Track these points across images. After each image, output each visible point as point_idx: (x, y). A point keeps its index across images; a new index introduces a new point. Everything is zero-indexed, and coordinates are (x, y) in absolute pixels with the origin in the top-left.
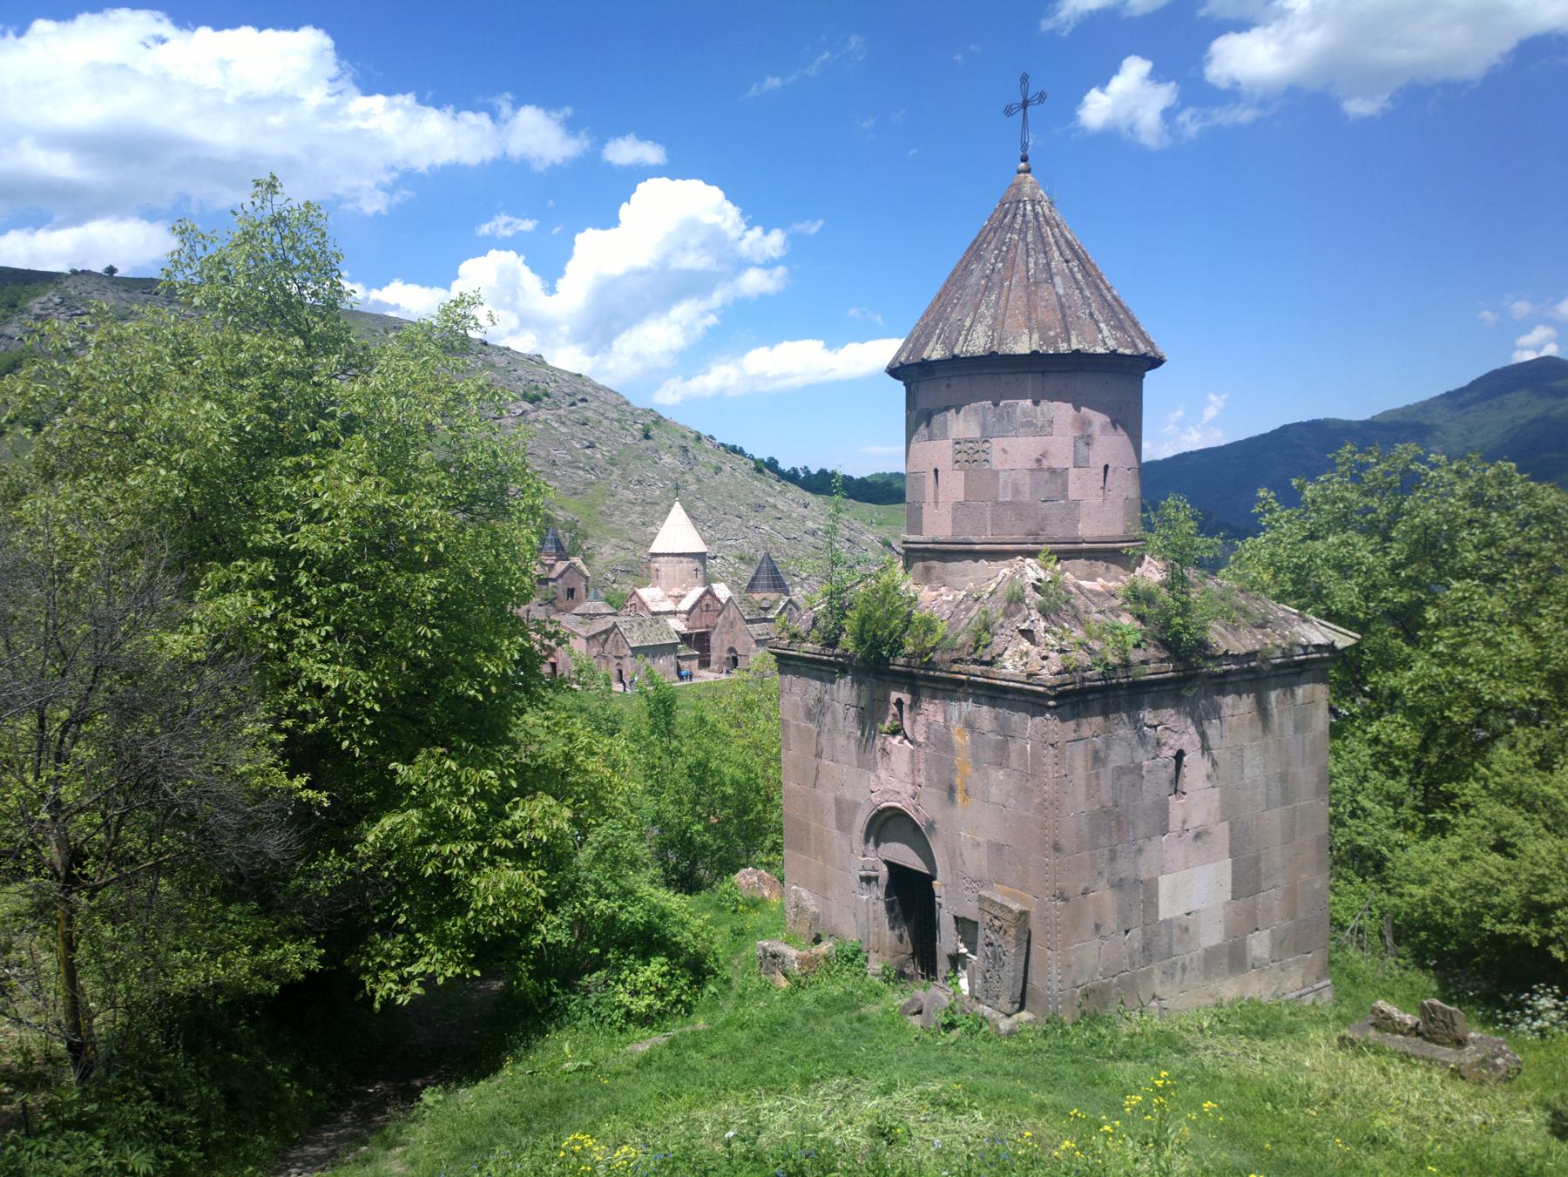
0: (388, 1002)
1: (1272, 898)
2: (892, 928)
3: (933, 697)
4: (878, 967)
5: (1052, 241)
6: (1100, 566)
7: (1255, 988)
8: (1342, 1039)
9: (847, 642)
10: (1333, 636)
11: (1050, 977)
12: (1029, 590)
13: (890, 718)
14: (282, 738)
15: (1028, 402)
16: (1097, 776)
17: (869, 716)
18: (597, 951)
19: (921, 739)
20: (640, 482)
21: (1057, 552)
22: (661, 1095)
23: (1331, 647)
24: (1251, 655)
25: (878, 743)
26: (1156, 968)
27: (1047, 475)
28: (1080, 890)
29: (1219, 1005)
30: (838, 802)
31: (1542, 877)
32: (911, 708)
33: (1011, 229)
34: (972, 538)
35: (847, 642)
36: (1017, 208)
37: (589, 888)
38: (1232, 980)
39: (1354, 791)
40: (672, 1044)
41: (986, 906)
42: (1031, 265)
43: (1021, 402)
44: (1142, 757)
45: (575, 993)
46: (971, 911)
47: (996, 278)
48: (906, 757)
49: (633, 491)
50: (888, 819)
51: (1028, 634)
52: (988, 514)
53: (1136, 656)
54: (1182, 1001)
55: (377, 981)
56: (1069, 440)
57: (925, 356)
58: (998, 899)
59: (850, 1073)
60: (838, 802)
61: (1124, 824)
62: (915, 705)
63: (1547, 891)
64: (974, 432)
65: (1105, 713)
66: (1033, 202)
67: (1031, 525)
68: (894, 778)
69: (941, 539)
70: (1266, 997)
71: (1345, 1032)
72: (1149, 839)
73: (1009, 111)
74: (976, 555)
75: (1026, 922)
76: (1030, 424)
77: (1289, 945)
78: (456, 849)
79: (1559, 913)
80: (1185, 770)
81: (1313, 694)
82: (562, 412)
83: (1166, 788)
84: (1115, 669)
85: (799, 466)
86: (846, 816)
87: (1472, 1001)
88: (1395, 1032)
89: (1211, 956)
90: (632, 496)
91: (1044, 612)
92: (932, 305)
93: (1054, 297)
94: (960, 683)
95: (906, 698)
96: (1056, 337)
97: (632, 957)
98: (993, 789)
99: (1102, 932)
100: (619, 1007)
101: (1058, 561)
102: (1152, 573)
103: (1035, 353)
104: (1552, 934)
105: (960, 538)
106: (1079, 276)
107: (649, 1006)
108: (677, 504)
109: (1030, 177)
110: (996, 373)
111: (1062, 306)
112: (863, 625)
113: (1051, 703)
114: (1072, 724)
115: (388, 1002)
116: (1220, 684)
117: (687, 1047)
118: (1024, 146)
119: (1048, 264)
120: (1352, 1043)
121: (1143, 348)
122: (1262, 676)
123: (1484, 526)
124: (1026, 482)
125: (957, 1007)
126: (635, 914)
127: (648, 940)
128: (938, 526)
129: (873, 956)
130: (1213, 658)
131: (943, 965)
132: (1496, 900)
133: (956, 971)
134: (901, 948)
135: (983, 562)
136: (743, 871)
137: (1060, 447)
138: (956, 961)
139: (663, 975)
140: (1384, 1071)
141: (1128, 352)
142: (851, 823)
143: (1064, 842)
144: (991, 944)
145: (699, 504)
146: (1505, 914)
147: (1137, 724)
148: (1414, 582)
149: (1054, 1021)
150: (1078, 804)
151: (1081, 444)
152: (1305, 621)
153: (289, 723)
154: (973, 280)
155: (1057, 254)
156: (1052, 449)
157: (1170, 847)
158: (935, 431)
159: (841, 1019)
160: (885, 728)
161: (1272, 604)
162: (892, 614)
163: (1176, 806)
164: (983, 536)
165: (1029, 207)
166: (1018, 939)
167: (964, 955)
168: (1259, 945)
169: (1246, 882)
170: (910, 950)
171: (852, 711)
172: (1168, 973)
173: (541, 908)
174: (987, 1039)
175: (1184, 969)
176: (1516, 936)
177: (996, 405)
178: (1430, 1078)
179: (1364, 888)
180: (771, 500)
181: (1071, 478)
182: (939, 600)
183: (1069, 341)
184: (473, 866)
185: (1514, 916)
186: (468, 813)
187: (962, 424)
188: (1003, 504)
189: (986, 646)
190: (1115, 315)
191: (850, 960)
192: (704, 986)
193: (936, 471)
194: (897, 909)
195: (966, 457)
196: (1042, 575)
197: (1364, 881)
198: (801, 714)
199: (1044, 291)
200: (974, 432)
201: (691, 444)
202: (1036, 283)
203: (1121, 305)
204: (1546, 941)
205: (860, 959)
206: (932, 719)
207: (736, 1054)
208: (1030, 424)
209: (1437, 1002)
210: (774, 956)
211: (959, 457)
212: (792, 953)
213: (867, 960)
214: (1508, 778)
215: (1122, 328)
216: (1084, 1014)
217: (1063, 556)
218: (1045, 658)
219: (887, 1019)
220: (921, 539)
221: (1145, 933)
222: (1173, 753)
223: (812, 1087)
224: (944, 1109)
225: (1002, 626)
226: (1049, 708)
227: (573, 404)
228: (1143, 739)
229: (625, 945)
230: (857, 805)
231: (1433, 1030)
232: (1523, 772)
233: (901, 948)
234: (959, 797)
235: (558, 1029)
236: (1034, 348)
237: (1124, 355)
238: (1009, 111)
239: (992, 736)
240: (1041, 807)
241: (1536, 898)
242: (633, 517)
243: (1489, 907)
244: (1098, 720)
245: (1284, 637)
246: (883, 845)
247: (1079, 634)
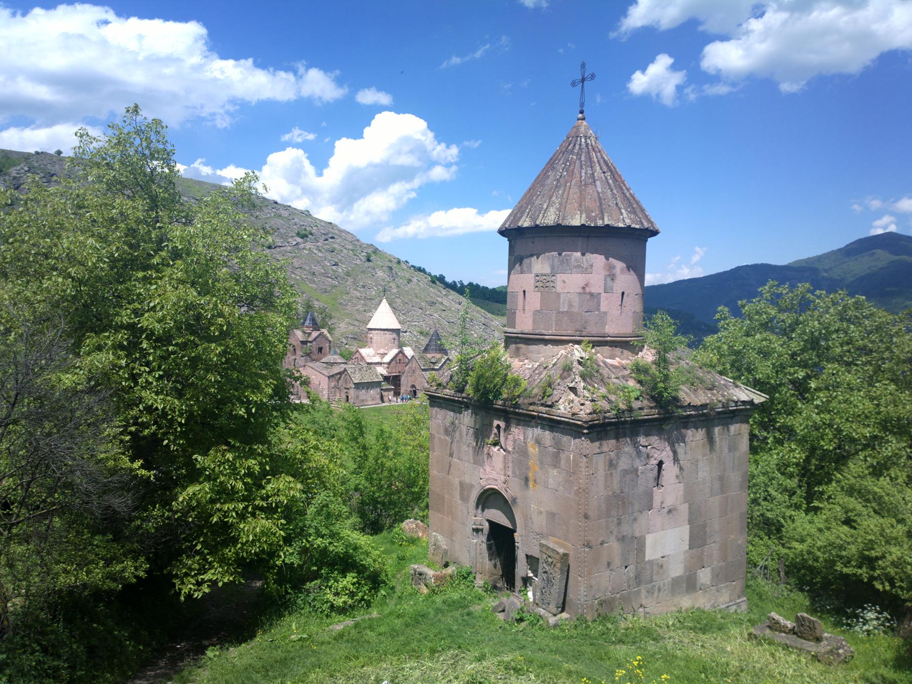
0: (189, 596)
1: (713, 548)
2: (490, 560)
3: (518, 425)
4: (481, 583)
5: (596, 160)
6: (618, 351)
7: (702, 601)
8: (750, 634)
9: (469, 390)
10: (753, 396)
11: (579, 592)
12: (575, 364)
13: (493, 436)
14: (128, 438)
15: (579, 254)
16: (611, 474)
17: (481, 434)
18: (315, 568)
19: (510, 449)
20: (364, 287)
21: (592, 342)
22: (347, 657)
23: (751, 402)
24: (704, 406)
25: (486, 450)
26: (643, 588)
27: (588, 297)
28: (600, 541)
29: (680, 612)
30: (461, 484)
31: (871, 540)
32: (505, 430)
33: (572, 152)
34: (544, 332)
35: (469, 390)
36: (576, 140)
37: (312, 531)
38: (688, 596)
39: (766, 485)
40: (356, 626)
41: (544, 550)
42: (583, 174)
43: (575, 254)
44: (639, 464)
45: (301, 593)
46: (535, 552)
48: (501, 459)
50: (490, 495)
51: (573, 390)
53: (636, 405)
54: (658, 609)
55: (183, 583)
57: (520, 224)
58: (551, 546)
59: (460, 647)
60: (461, 484)
61: (627, 504)
62: (507, 428)
63: (873, 549)
64: (547, 270)
65: (617, 438)
66: (586, 137)
68: (493, 472)
69: (526, 331)
70: (707, 607)
71: (752, 630)
72: (641, 512)
73: (574, 84)
74: (546, 342)
75: (567, 560)
76: (579, 266)
79: (880, 562)
80: (663, 472)
81: (740, 430)
82: (319, 244)
83: (652, 483)
84: (623, 412)
85: (457, 280)
86: (466, 493)
87: (829, 612)
89: (676, 582)
90: (359, 294)
91: (583, 377)
92: (525, 195)
93: (596, 193)
94: (533, 417)
95: (502, 424)
96: (596, 216)
97: (336, 572)
98: (551, 481)
99: (612, 567)
100: (327, 602)
101: (593, 347)
102: (648, 356)
103: (583, 225)
104: (876, 575)
105: (537, 332)
106: (611, 181)
107: (345, 602)
108: (384, 300)
109: (584, 123)
110: (560, 236)
111: (600, 199)
112: (479, 380)
113: (585, 431)
114: (597, 444)
115: (189, 596)
116: (685, 422)
117: (365, 628)
118: (582, 105)
119: (593, 174)
120: (756, 638)
121: (646, 225)
122: (711, 418)
123: (846, 333)
124: (576, 300)
125: (525, 609)
126: (338, 548)
127: (346, 563)
128: (524, 324)
129: (478, 576)
130: (682, 407)
131: (519, 583)
132: (844, 553)
133: (526, 587)
134: (495, 571)
135: (550, 346)
136: (407, 521)
137: (597, 281)
138: (526, 581)
139: (353, 584)
140: (773, 655)
141: (637, 227)
142: (468, 497)
143: (590, 513)
144: (546, 572)
145: (397, 300)
146: (849, 562)
147: (636, 445)
148: (804, 365)
149: (581, 620)
150: (599, 491)
151: (609, 279)
152: (737, 386)
153: (133, 429)
154: (549, 181)
155: (598, 168)
156: (592, 282)
157: (653, 517)
158: (525, 268)
159: (457, 614)
160: (490, 442)
161: (717, 376)
162: (496, 374)
164: (550, 331)
165: (583, 140)
166: (561, 570)
167: (531, 578)
168: (704, 576)
169: (698, 539)
170: (501, 573)
171: (471, 431)
172: (650, 592)
173: (281, 543)
174: (542, 629)
175: (659, 590)
176: (854, 575)
177: (560, 254)
178: (799, 661)
179: (769, 542)
180: (440, 299)
181: (602, 299)
182: (523, 367)
183: (603, 219)
184: (242, 516)
185: (854, 563)
186: (240, 485)
187: (540, 265)
188: (562, 313)
189: (549, 396)
190: (631, 205)
191: (465, 578)
192: (379, 591)
193: (524, 292)
194: (494, 548)
195: (541, 284)
196: (583, 355)
197: (770, 538)
198: (442, 431)
199: (590, 189)
200: (547, 270)
201: (394, 265)
202: (585, 185)
203: (634, 199)
204: (872, 578)
205: (471, 578)
206: (517, 437)
207: (393, 634)
208: (579, 266)
209: (805, 615)
210: (420, 574)
211: (537, 284)
212: (430, 573)
213: (475, 578)
214: (853, 481)
215: (635, 213)
216: (599, 615)
217: (595, 344)
218: (582, 405)
219: (484, 615)
220: (514, 331)
221: (637, 568)
222: (656, 462)
223: (436, 655)
224: (512, 672)
225: (559, 384)
226: (584, 434)
227: (326, 240)
228: (639, 453)
229: (332, 565)
230: (472, 486)
231: (803, 631)
232: (862, 478)
233: (495, 571)
234: (531, 484)
235: (290, 614)
236: (583, 222)
237: (635, 229)
238: (574, 84)
239: (551, 449)
240: (577, 493)
241: (867, 553)
242: (359, 306)
243: (841, 557)
244: (613, 442)
245: (723, 396)
246: (486, 510)
247: (603, 391)
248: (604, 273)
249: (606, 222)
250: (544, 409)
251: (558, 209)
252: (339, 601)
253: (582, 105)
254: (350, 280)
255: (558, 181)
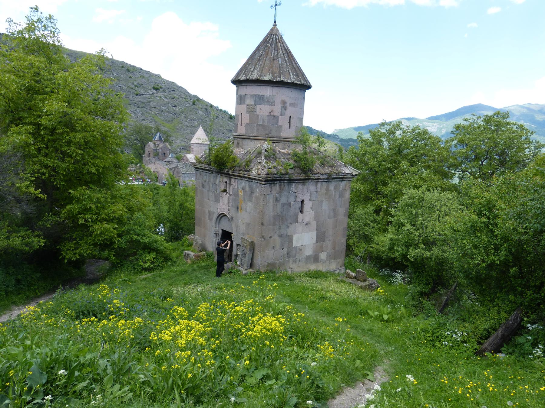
1: (328, 243)
7: (322, 268)
11: (258, 261)
12: (263, 151)
14: (33, 179)
16: (277, 205)
19: (231, 193)
20: (191, 120)
23: (351, 174)
27: (272, 117)
29: (309, 271)
30: (209, 212)
47: (262, 57)
48: (227, 199)
49: (188, 122)
52: (255, 128)
55: (67, 254)
56: (280, 107)
57: (239, 78)
60: (209, 212)
61: (284, 219)
67: (267, 132)
68: (223, 205)
73: (272, 7)
77: (333, 256)
78: (89, 217)
82: (166, 94)
83: (298, 210)
88: (350, 278)
89: (308, 258)
90: (188, 124)
91: (266, 157)
96: (277, 76)
98: (248, 208)
106: (286, 59)
108: (201, 127)
118: (275, 18)
121: (303, 82)
128: (242, 130)
139: (154, 258)
141: (298, 83)
143: (265, 223)
150: (270, 212)
151: (283, 109)
152: (345, 166)
153: (36, 175)
157: (299, 227)
163: (300, 216)
164: (253, 134)
166: (250, 249)
169: (321, 238)
172: (295, 261)
173: (115, 236)
175: (299, 261)
182: (239, 152)
184: (94, 222)
186: (94, 207)
188: (260, 125)
190: (296, 71)
198: (201, 186)
201: (209, 108)
202: (273, 60)
208: (268, 101)
210: (188, 255)
212: (192, 254)
220: (237, 134)
227: (170, 92)
230: (214, 213)
240: (259, 213)
245: (337, 170)
247: (275, 164)
248: (281, 106)
249: (282, 79)
250: (246, 173)
251: (259, 72)
252: (146, 266)
253: (275, 18)
254: (183, 115)
255: (260, 57)
